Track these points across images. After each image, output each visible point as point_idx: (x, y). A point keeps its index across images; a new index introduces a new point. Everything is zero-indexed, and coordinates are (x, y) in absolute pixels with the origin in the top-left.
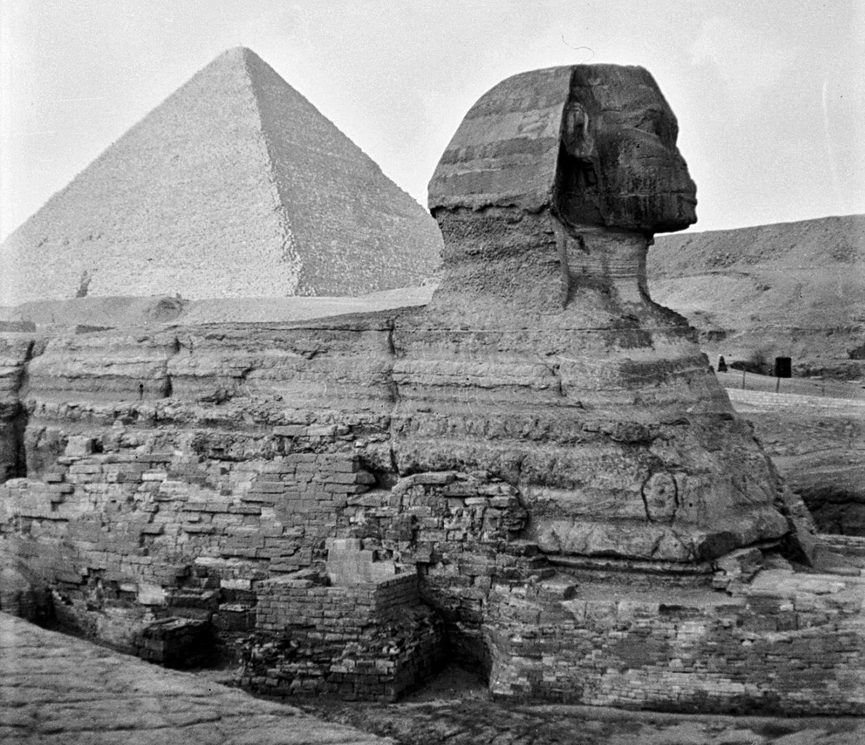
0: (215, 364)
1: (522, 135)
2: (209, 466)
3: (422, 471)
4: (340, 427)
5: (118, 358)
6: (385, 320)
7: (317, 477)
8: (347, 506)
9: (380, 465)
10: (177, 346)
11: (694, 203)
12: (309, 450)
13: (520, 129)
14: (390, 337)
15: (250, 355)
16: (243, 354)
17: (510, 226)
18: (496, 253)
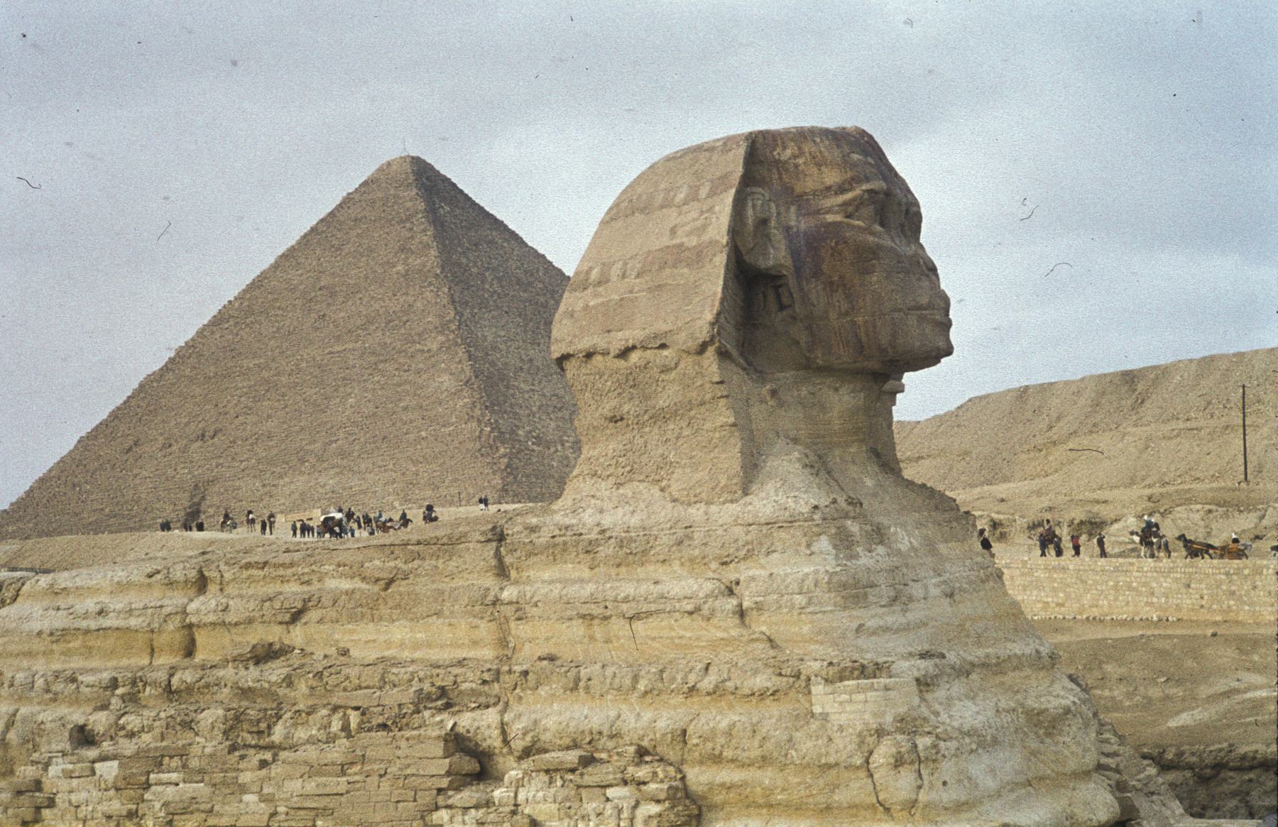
0: (252, 605)
1: (677, 241)
2: (242, 757)
3: (546, 751)
4: (427, 687)
5: (118, 604)
6: (490, 526)
7: (393, 769)
8: (437, 808)
9: (485, 745)
10: (201, 584)
11: (948, 324)
12: (384, 726)
13: (673, 231)
14: (498, 550)
15: (306, 588)
16: (293, 588)
17: (663, 376)
18: (646, 417)
